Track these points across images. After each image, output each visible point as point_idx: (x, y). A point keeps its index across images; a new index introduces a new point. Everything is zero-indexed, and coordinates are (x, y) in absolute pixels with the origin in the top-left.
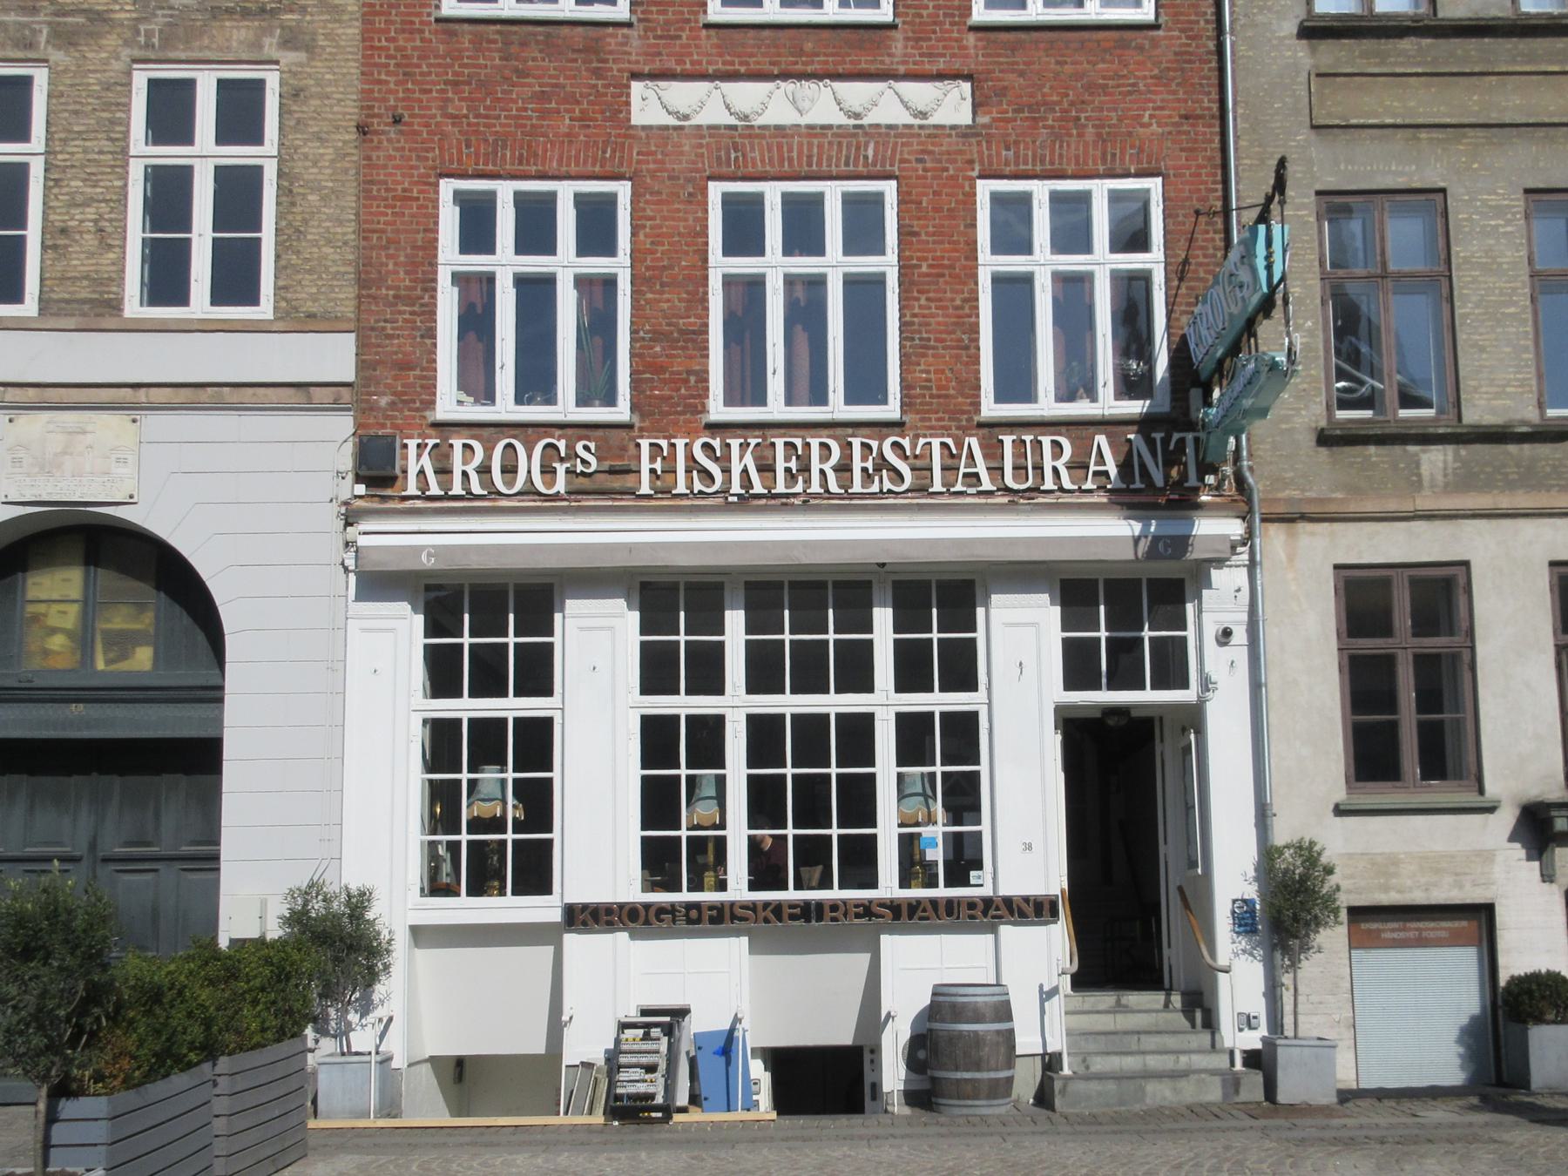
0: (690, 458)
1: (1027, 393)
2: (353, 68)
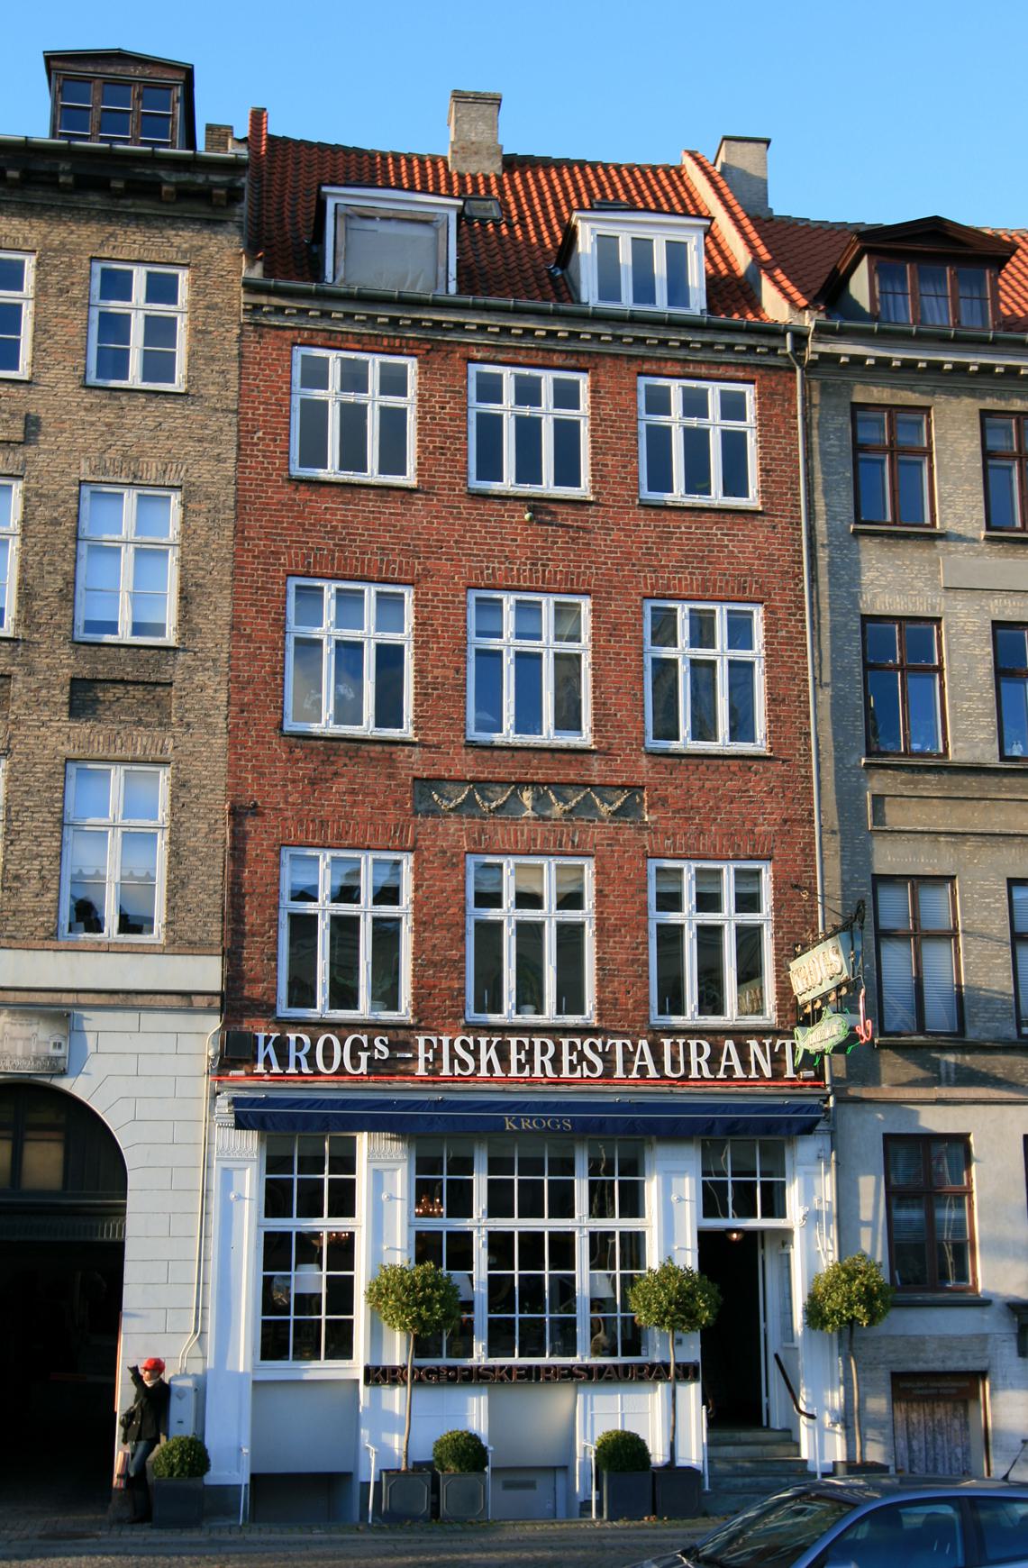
0: (452, 1048)
1: (679, 1009)
2: (222, 767)
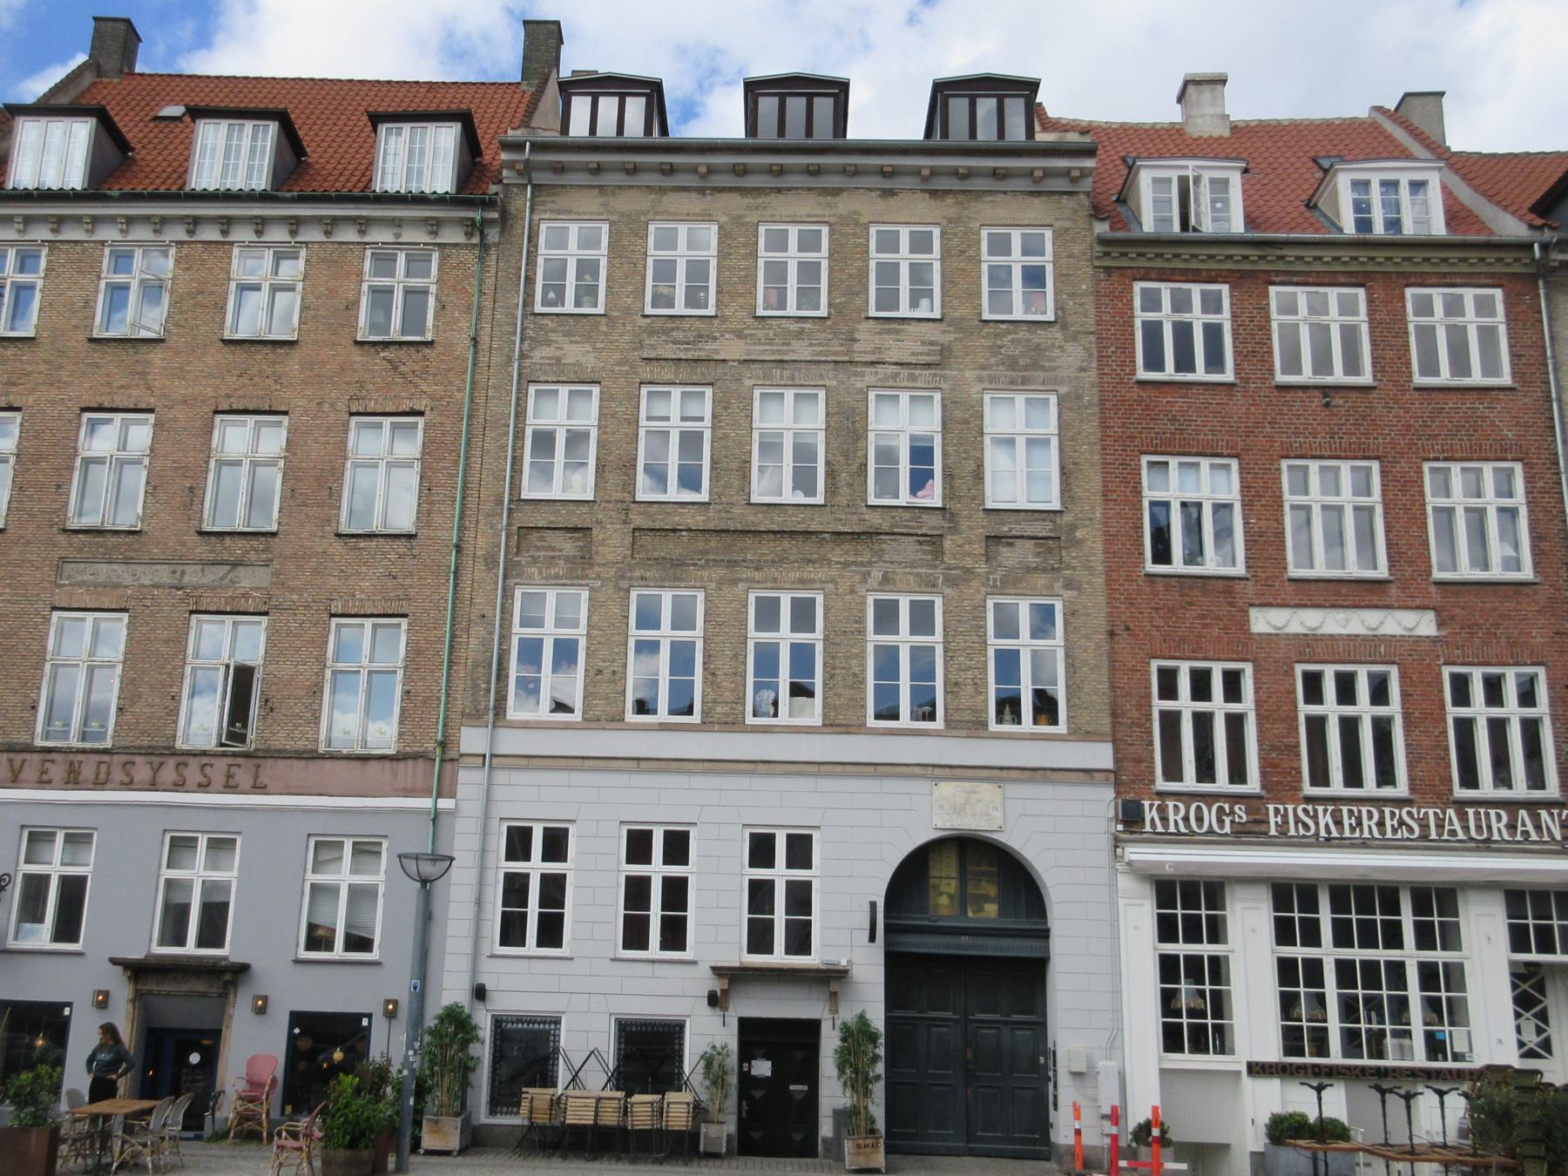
2: (1102, 600)
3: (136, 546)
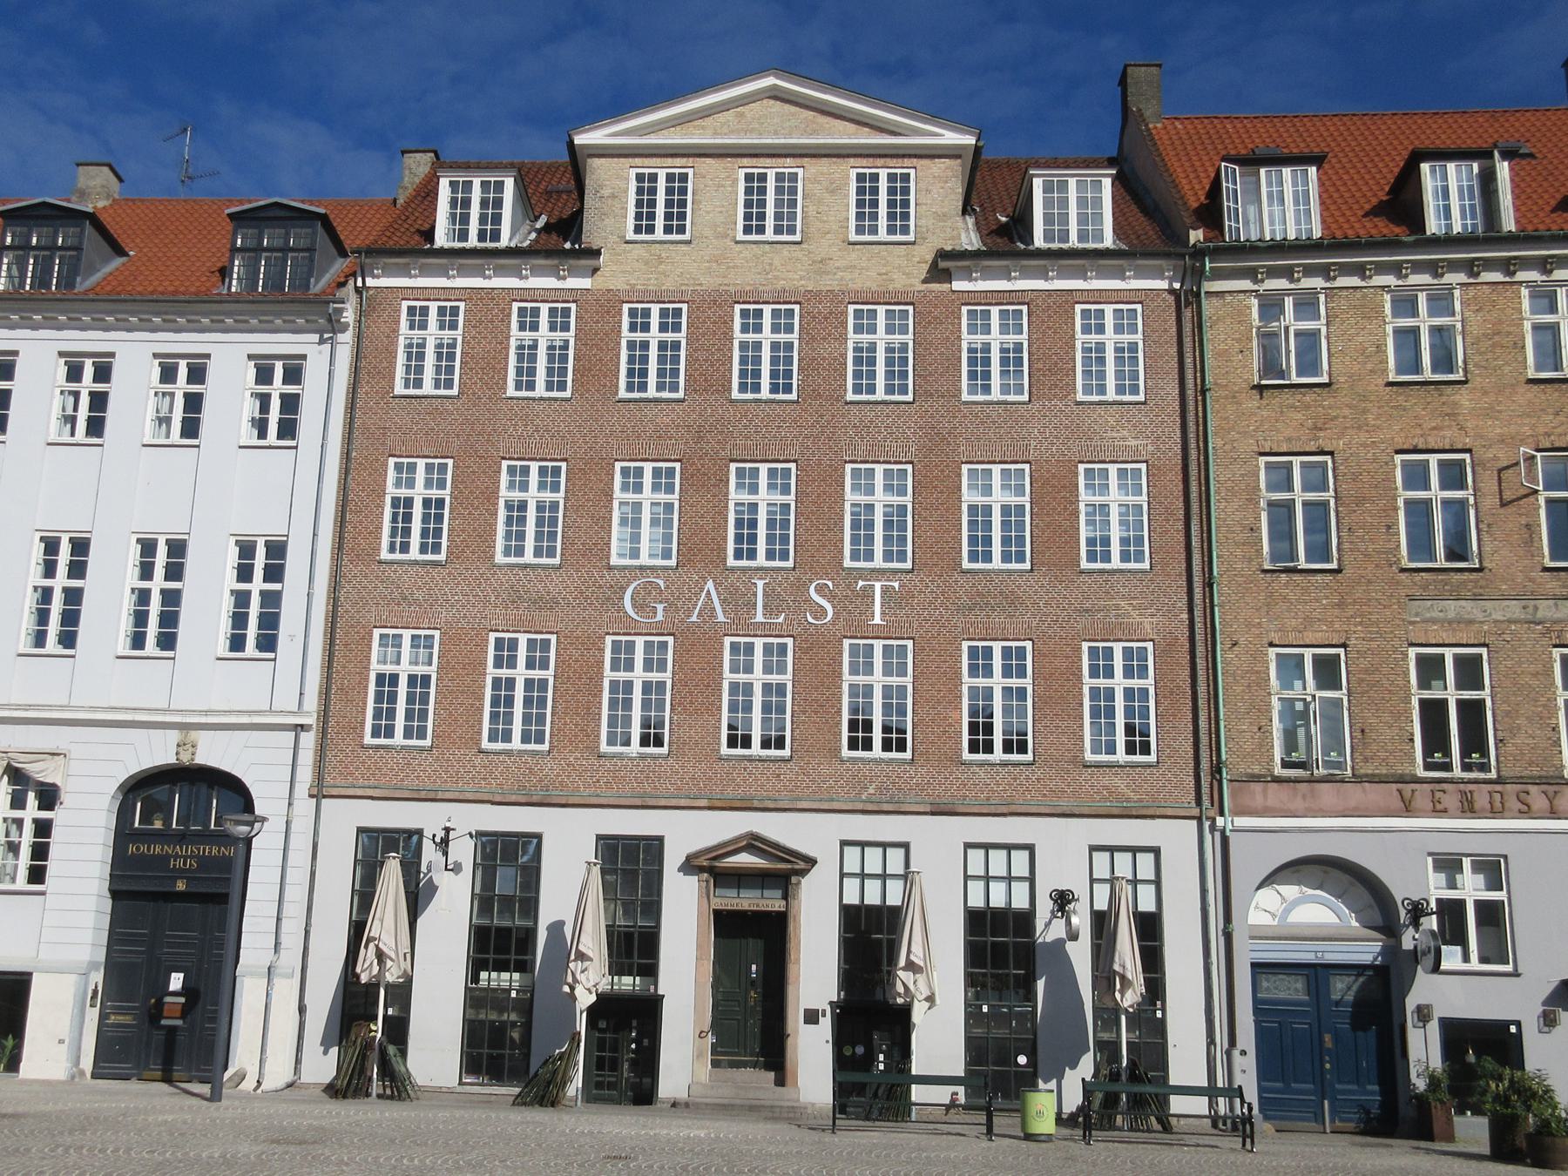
3: (1482, 583)
